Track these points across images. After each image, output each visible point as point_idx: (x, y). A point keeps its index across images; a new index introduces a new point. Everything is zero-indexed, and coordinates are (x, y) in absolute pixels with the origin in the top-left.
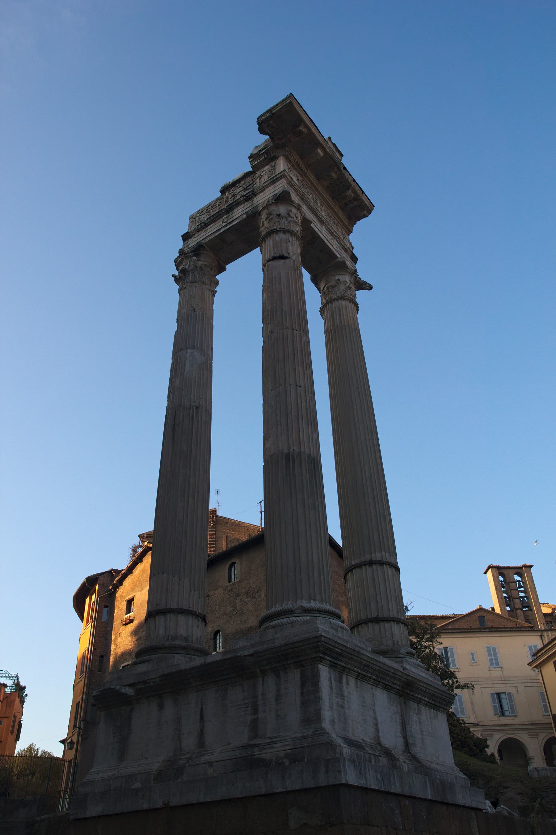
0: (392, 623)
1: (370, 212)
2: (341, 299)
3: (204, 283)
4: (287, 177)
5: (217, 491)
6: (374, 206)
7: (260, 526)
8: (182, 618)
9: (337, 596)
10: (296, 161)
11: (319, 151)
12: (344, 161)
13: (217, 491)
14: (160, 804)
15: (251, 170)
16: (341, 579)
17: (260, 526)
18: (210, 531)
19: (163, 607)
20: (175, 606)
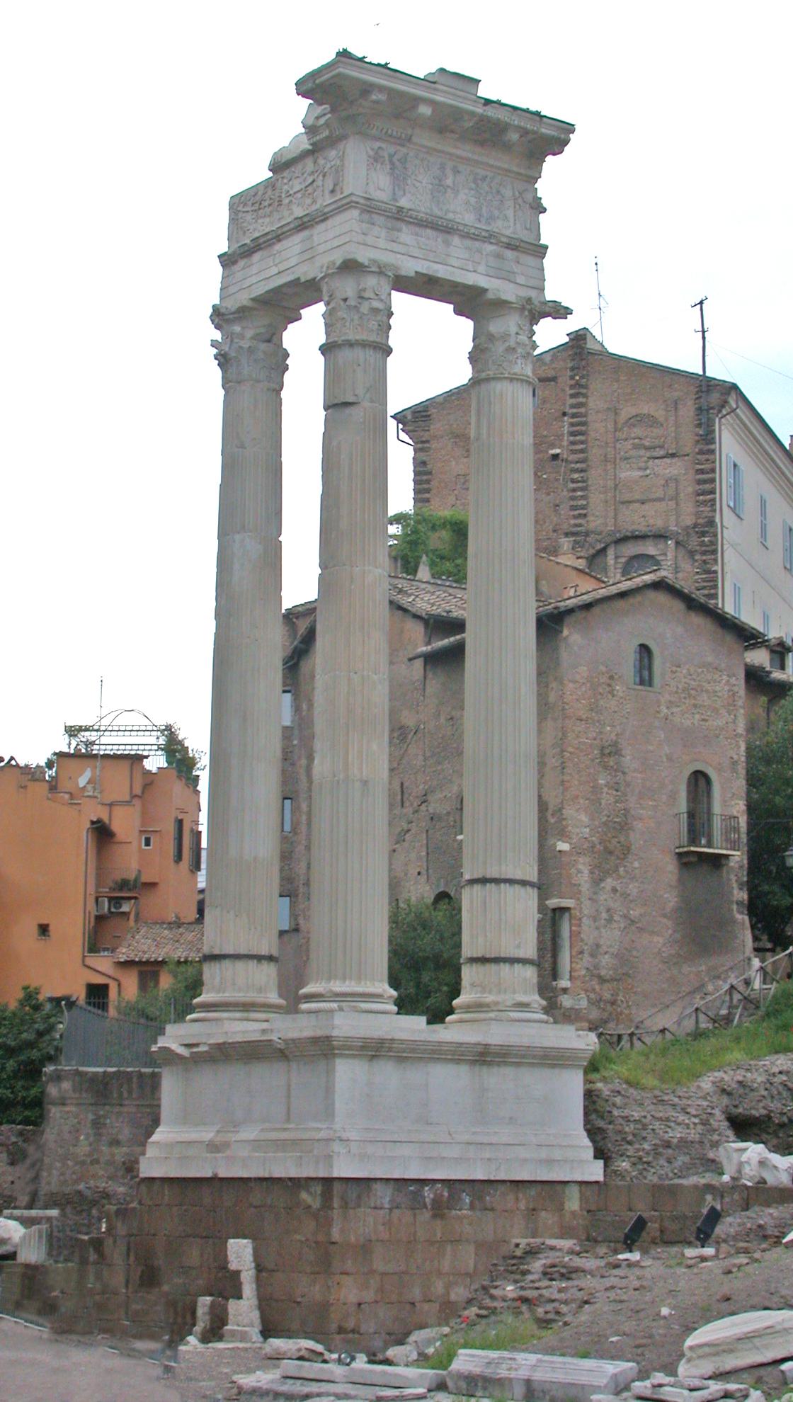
0: (502, 964)
1: (566, 142)
2: (493, 379)
3: (258, 381)
4: (357, 203)
5: (596, 264)
6: (573, 125)
7: (701, 373)
8: (240, 965)
9: (703, 720)
10: (385, 130)
11: (425, 110)
12: (484, 91)
13: (596, 264)
14: (209, 1175)
15: (310, 147)
16: (720, 676)
17: (701, 373)
18: (572, 396)
19: (217, 952)
20: (232, 952)
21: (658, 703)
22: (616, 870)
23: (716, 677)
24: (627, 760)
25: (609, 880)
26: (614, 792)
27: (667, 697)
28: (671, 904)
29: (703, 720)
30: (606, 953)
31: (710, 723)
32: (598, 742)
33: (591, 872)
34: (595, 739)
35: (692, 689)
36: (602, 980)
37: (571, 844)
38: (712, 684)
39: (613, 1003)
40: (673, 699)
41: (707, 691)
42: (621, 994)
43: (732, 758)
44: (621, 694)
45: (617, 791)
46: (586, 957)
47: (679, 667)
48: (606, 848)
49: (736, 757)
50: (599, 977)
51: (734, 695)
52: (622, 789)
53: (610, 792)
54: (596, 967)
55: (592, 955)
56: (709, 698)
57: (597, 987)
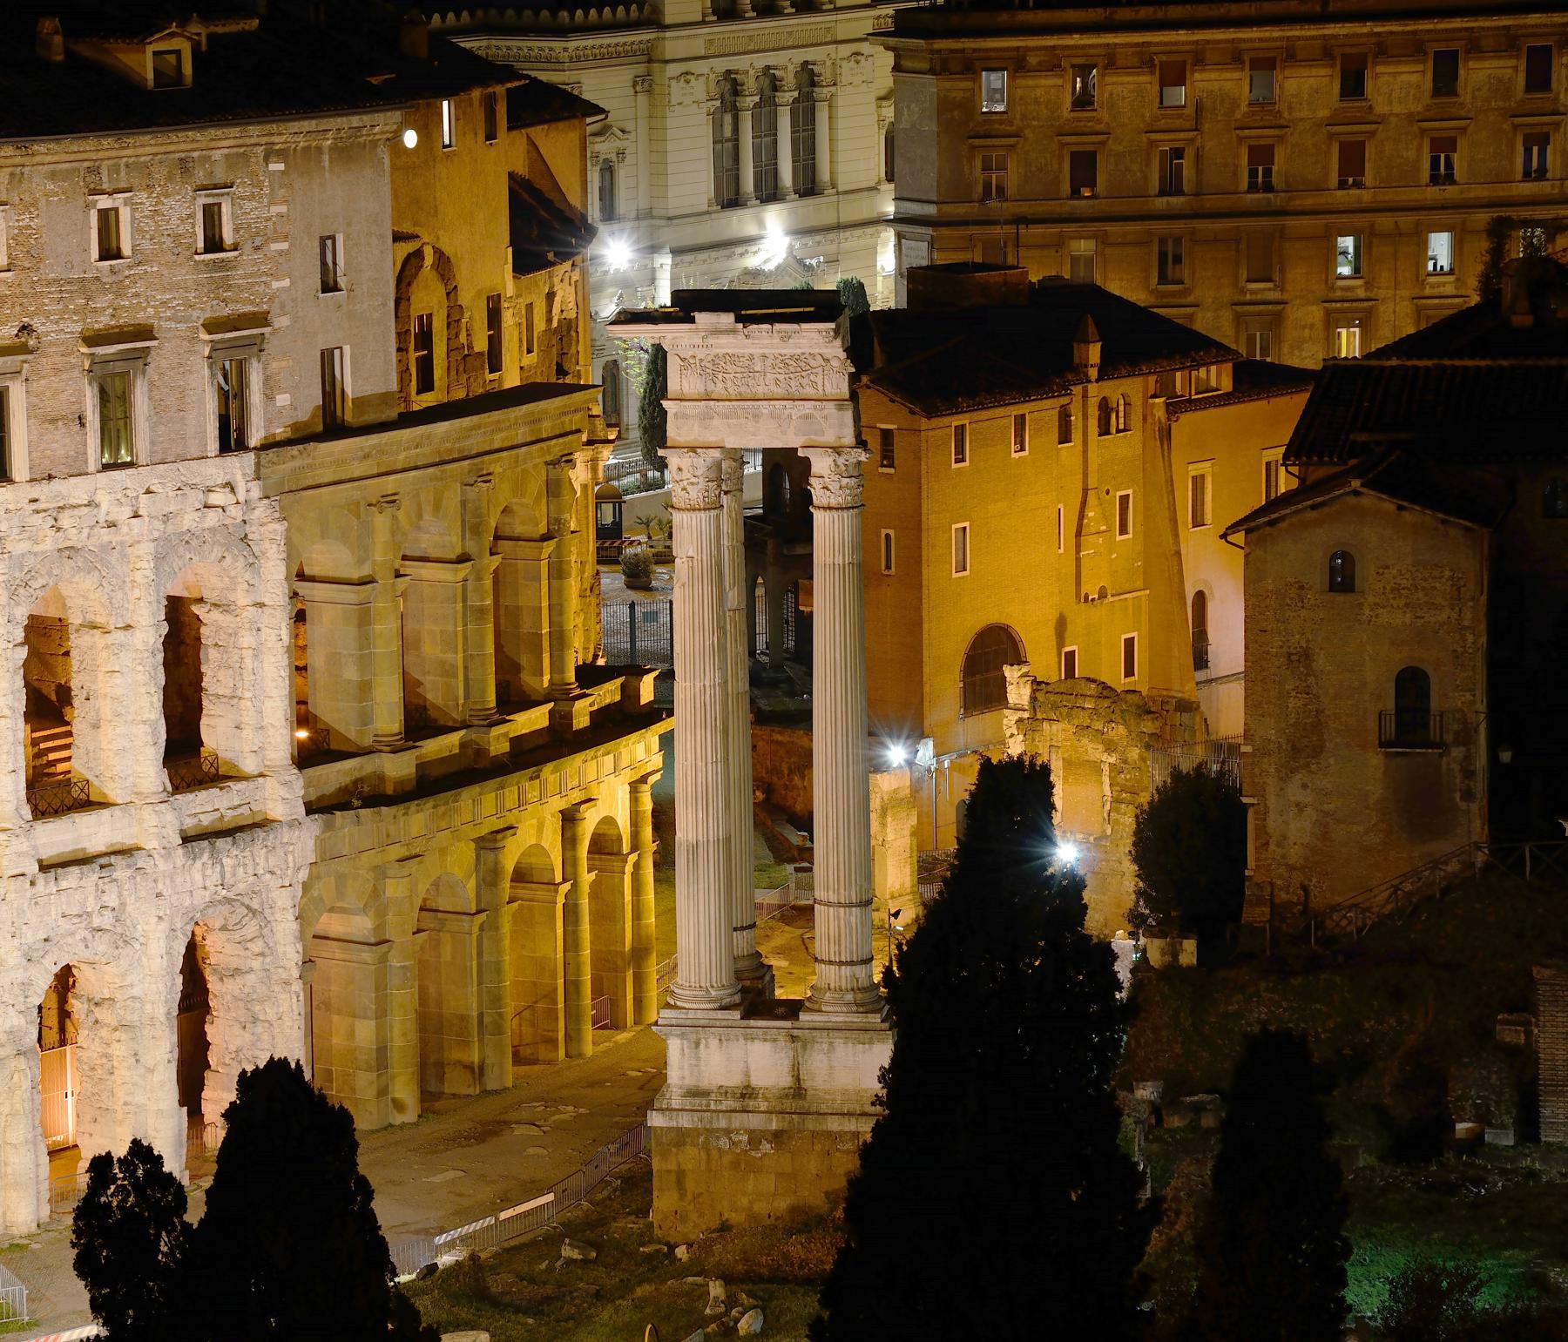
9: (1417, 617)
21: (1361, 604)
22: (1307, 765)
23: (1436, 573)
24: (1320, 661)
25: (1299, 776)
26: (1305, 696)
27: (1371, 599)
28: (1377, 795)
29: (1417, 617)
30: (1295, 844)
31: (1425, 619)
32: (1285, 649)
33: (1278, 771)
34: (1281, 647)
35: (1403, 589)
36: (1291, 868)
37: (1253, 746)
38: (1430, 581)
39: (1305, 888)
40: (1377, 600)
41: (1423, 589)
42: (1314, 880)
43: (1455, 651)
44: (1312, 602)
45: (1308, 694)
46: (1272, 847)
47: (1388, 567)
48: (1294, 748)
49: (1459, 649)
50: (1287, 865)
51: (1459, 589)
52: (1314, 692)
53: (1299, 695)
54: (1284, 857)
55: (1278, 846)
56: (1426, 595)
57: (1286, 875)
